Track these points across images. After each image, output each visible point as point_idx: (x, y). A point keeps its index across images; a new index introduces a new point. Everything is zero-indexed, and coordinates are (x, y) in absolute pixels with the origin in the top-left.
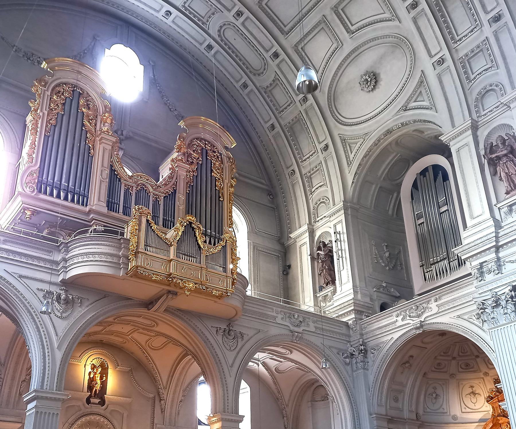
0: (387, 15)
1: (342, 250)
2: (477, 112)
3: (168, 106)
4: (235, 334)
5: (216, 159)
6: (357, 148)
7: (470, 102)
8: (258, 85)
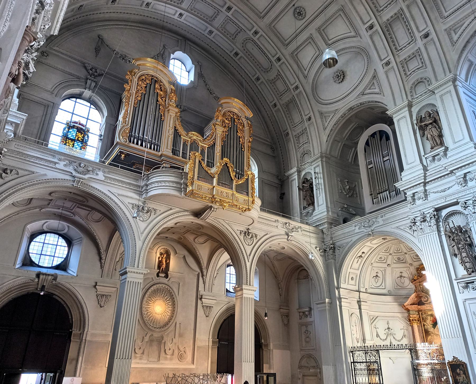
0: (353, 34)
1: (319, 184)
2: (412, 96)
4: (252, 235)
6: (330, 119)
7: (407, 90)
8: (266, 79)
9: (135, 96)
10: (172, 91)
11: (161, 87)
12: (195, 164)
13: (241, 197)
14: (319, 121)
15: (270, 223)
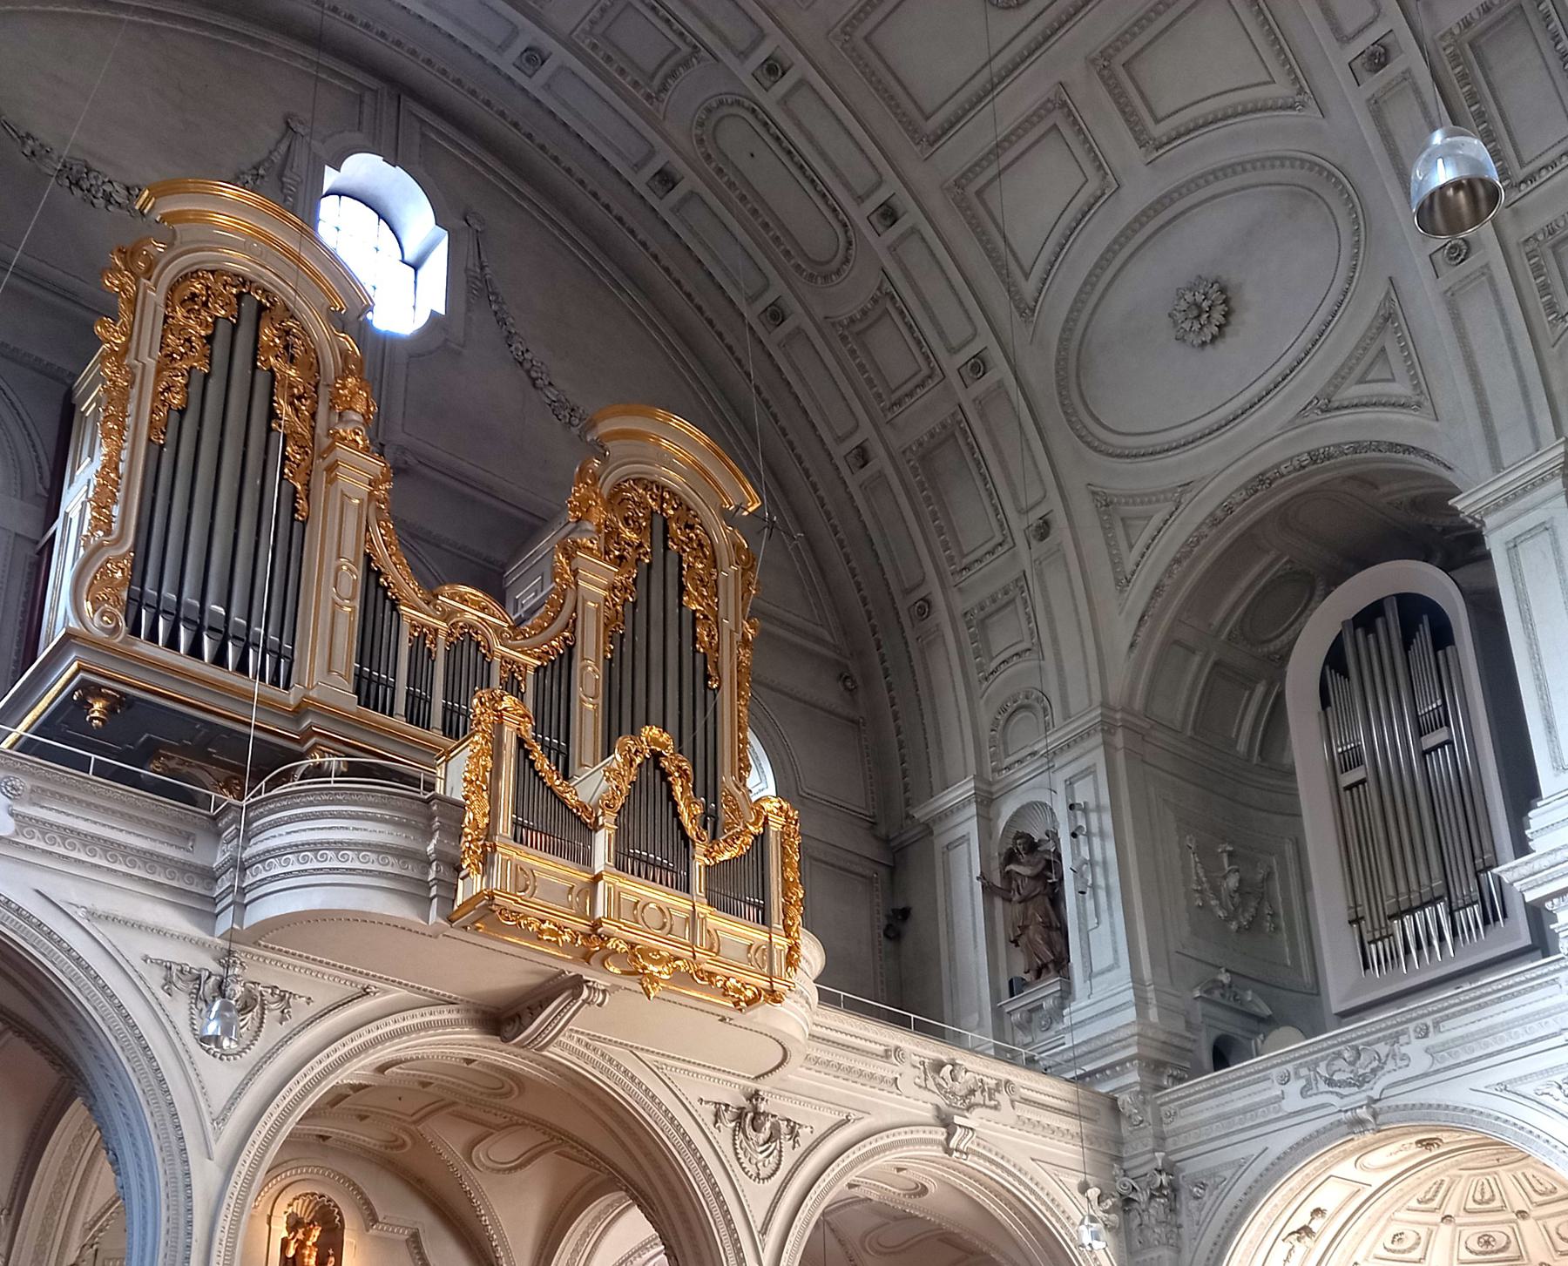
1: (1092, 863)
3: (528, 372)
4: (775, 1128)
5: (694, 549)
6: (1150, 530)
9: (156, 384)
10: (345, 362)
11: (290, 338)
12: (497, 756)
13: (737, 932)
14: (1094, 541)
15: (859, 1063)
